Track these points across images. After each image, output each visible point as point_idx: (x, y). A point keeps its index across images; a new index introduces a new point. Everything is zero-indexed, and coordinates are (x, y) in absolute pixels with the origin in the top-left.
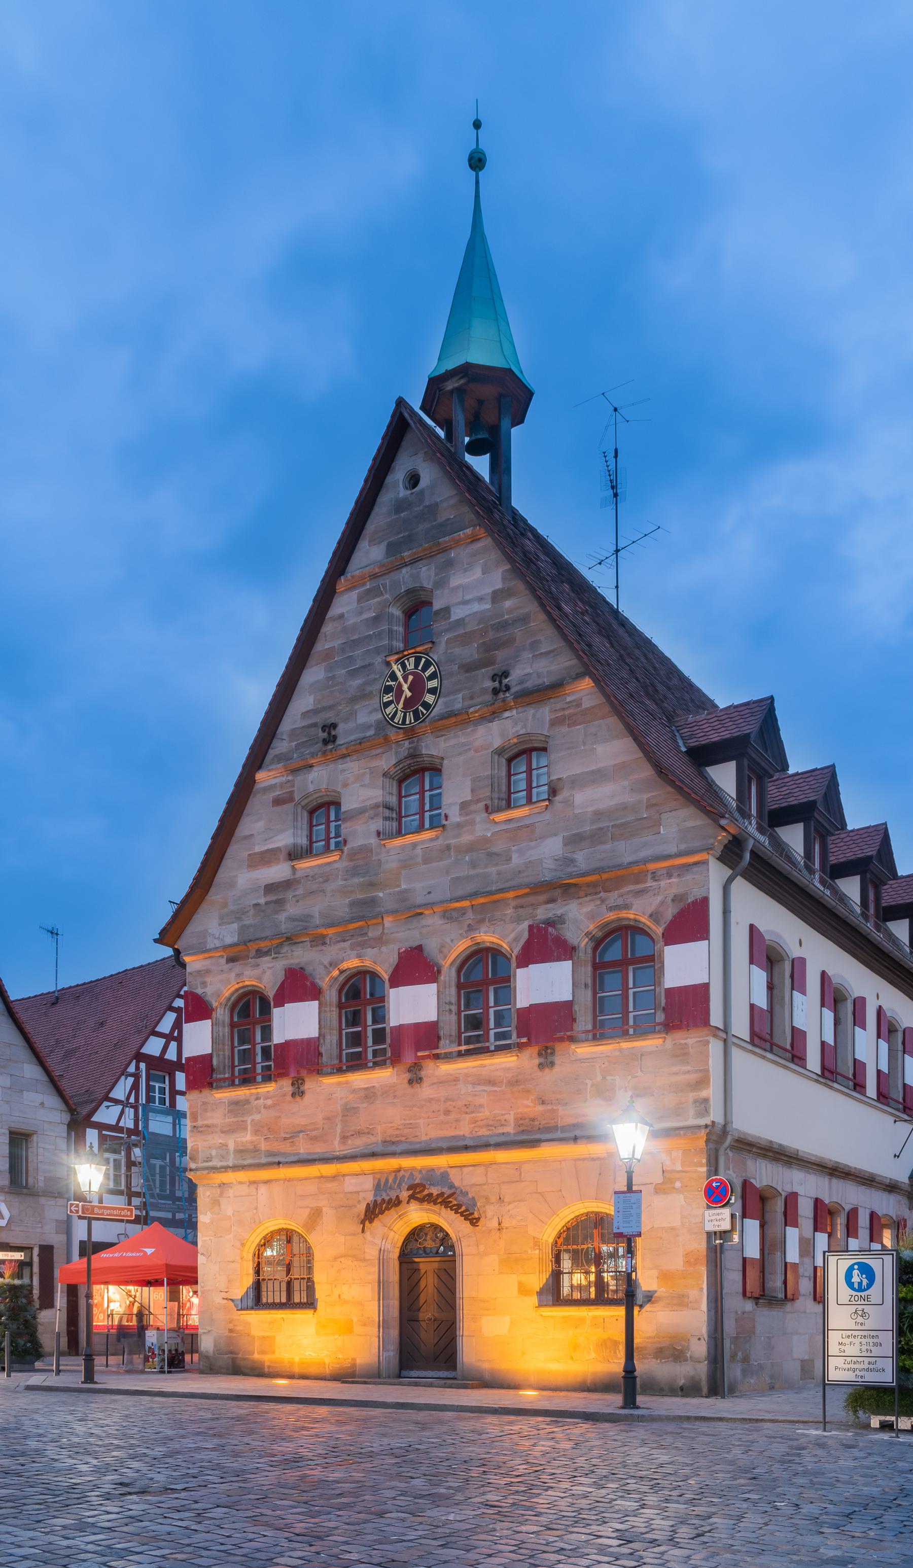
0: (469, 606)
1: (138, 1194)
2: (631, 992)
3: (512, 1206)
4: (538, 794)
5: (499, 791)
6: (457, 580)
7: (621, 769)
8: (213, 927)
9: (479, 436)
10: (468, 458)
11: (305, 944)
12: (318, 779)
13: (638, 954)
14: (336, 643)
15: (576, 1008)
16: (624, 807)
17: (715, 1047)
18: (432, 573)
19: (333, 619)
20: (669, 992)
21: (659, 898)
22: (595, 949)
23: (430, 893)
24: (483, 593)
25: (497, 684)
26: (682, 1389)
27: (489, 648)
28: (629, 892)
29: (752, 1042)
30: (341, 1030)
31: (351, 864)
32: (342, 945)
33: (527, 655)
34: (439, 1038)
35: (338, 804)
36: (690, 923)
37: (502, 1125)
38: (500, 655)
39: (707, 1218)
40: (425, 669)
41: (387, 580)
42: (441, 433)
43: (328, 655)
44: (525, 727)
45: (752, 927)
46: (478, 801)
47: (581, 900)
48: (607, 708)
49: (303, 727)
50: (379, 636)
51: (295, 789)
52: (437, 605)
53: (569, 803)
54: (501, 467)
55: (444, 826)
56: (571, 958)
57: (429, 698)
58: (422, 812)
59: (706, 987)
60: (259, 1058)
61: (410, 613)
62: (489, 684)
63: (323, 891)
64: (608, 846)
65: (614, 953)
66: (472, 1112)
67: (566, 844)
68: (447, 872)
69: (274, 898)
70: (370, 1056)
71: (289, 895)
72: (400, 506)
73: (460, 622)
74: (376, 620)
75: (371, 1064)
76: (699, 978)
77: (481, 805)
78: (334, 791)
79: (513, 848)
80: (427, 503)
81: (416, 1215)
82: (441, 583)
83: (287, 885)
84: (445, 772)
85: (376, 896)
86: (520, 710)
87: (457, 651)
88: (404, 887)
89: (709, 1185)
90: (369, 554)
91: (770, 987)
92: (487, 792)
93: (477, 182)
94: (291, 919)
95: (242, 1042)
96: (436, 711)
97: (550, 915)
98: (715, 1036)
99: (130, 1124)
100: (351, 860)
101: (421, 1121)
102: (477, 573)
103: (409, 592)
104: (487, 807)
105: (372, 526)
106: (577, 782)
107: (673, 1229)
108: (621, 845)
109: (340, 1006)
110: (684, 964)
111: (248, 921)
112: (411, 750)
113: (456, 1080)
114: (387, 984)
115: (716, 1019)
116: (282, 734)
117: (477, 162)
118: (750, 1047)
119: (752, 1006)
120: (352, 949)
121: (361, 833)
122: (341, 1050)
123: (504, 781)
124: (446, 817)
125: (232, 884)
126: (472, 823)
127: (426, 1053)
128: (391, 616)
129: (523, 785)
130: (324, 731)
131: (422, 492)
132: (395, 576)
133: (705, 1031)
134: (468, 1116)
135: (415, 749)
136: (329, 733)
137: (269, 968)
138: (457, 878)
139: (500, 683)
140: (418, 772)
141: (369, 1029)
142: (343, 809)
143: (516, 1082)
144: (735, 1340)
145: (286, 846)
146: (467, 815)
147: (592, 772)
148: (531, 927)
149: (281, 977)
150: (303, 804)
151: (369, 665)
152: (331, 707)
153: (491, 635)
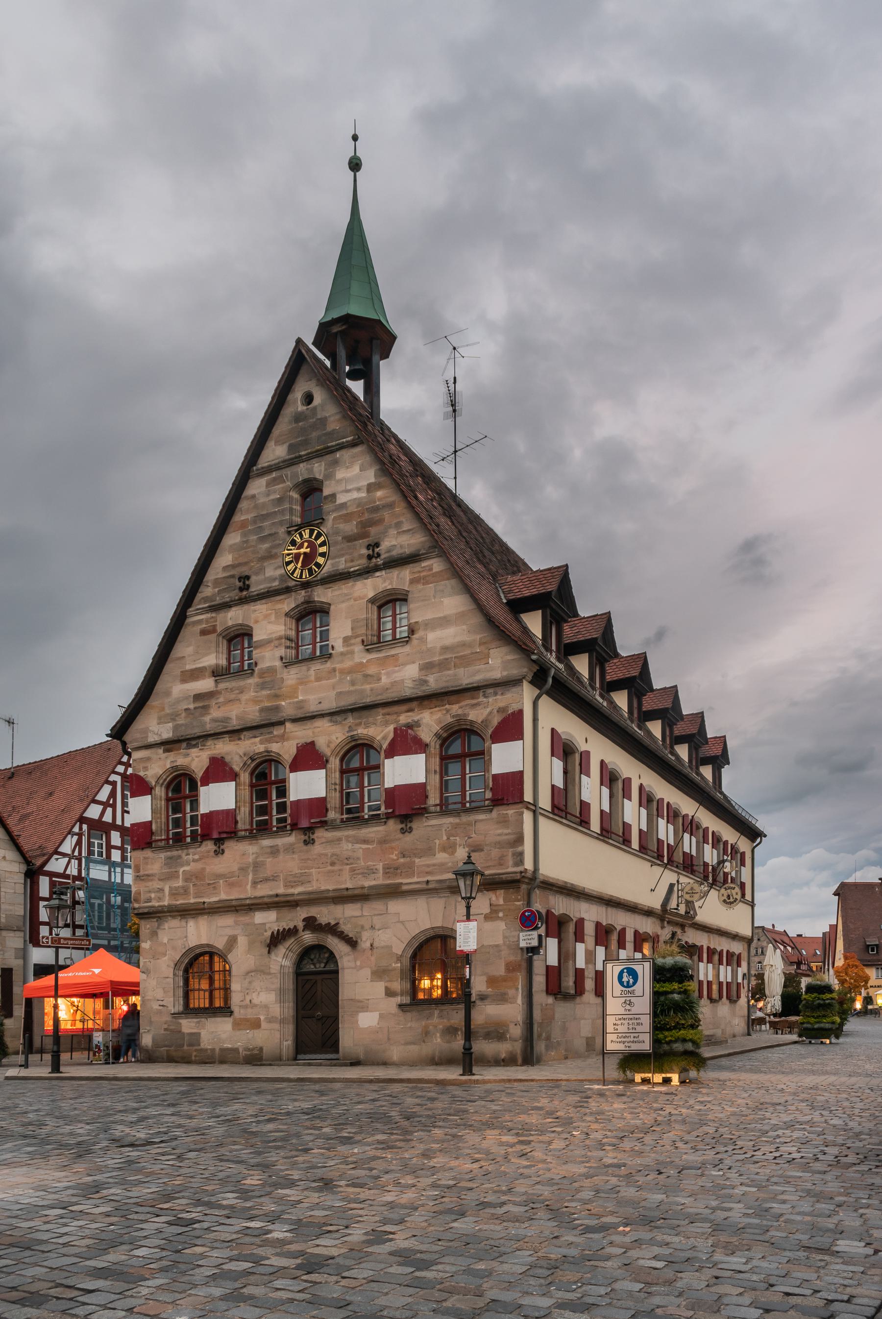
0: (350, 494)
1: (81, 927)
2: (468, 776)
4: (400, 632)
5: (372, 629)
6: (340, 474)
7: (460, 617)
8: (153, 726)
9: (357, 367)
10: (349, 383)
12: (234, 617)
13: (473, 749)
14: (249, 516)
15: (428, 788)
16: (463, 645)
17: (528, 817)
18: (323, 468)
19: (247, 498)
20: (495, 777)
21: (488, 710)
22: (441, 746)
24: (360, 484)
25: (370, 552)
26: (503, 1060)
27: (365, 525)
28: (466, 705)
29: (553, 812)
30: (252, 803)
31: (261, 680)
33: (393, 532)
34: (327, 810)
35: (250, 635)
36: (510, 728)
38: (373, 530)
39: (521, 938)
40: (317, 538)
41: (288, 472)
42: (328, 363)
43: (244, 524)
44: (391, 583)
45: (553, 730)
50: (282, 512)
52: (326, 492)
53: (423, 640)
54: (372, 390)
55: (331, 654)
56: (425, 752)
57: (320, 560)
58: (314, 644)
59: (521, 774)
60: (188, 825)
61: (305, 496)
62: (364, 551)
63: (239, 700)
65: (456, 748)
66: (352, 864)
67: (421, 670)
68: (334, 688)
69: (201, 704)
70: (275, 823)
71: (213, 702)
72: (298, 418)
73: (343, 505)
74: (280, 501)
75: (275, 829)
76: (518, 767)
77: (359, 640)
78: (248, 626)
80: (319, 417)
81: (308, 938)
82: (329, 476)
83: (210, 695)
84: (331, 613)
86: (388, 571)
87: (341, 526)
88: (300, 698)
89: (523, 914)
90: (275, 452)
91: (565, 772)
92: (363, 631)
94: (214, 720)
95: (174, 812)
96: (326, 569)
97: (410, 721)
98: (528, 808)
99: (75, 872)
100: (260, 677)
101: (313, 870)
102: (356, 469)
103: (306, 481)
104: (363, 641)
105: (277, 431)
106: (431, 625)
107: (497, 946)
108: (461, 671)
109: (252, 786)
110: (505, 758)
111: (181, 721)
113: (339, 839)
114: (288, 769)
115: (528, 797)
116: (208, 582)
118: (551, 816)
119: (553, 786)
120: (261, 743)
121: (269, 658)
122: (252, 818)
123: (376, 622)
124: (333, 647)
125: (168, 694)
126: (352, 653)
127: (318, 820)
128: (291, 498)
129: (389, 626)
130: (240, 581)
131: (315, 408)
132: (294, 469)
133: (520, 805)
135: (309, 596)
136: (244, 583)
138: (341, 693)
139: (373, 551)
140: (311, 613)
141: (274, 803)
142: (255, 639)
143: (383, 841)
144: (540, 1025)
145: (210, 666)
146: (348, 646)
147: (440, 618)
148: (395, 729)
149: (206, 763)
152: (246, 563)
153: (367, 516)
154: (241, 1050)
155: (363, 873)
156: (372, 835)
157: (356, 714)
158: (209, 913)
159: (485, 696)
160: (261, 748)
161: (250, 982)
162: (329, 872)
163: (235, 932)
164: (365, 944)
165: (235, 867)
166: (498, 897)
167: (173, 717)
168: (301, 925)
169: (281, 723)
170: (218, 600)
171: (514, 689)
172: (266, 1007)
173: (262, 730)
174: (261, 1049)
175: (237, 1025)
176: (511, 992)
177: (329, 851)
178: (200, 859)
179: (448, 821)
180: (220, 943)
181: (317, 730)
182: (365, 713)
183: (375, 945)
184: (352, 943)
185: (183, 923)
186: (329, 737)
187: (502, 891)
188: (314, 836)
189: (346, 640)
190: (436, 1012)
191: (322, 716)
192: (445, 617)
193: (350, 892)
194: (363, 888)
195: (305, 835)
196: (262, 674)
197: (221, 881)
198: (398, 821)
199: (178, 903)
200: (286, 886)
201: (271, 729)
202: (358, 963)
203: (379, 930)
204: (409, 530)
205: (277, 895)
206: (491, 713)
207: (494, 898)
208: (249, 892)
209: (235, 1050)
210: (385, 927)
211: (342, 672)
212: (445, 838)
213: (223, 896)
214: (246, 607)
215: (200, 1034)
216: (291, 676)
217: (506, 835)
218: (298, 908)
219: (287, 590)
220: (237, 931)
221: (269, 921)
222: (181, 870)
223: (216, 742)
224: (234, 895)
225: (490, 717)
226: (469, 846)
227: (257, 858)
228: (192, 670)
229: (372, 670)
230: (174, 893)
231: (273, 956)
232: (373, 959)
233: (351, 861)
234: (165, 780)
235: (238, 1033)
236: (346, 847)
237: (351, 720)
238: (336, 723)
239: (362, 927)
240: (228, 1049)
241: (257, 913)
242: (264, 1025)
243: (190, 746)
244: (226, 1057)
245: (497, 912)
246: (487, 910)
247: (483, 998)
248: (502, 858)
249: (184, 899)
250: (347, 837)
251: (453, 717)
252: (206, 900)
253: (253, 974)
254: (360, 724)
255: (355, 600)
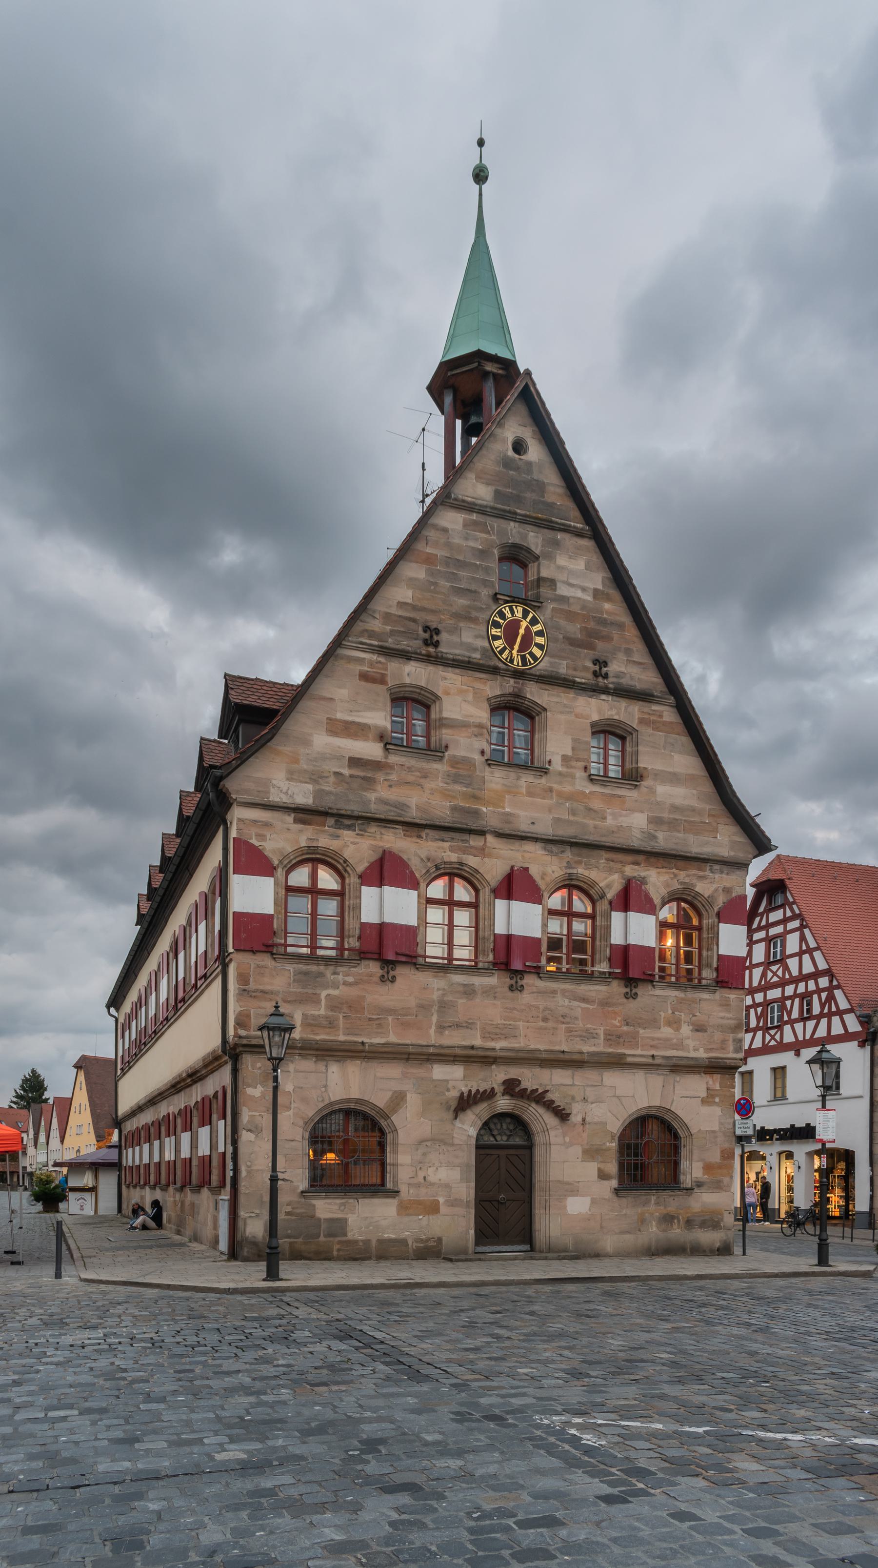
0: (573, 590)
3: (594, 1105)
11: (398, 831)
12: (414, 674)
16: (693, 810)
21: (714, 886)
23: (533, 823)
32: (441, 844)
37: (594, 1038)
41: (496, 523)
43: (429, 560)
46: (578, 760)
47: (659, 870)
48: (681, 728)
49: (400, 616)
51: (388, 673)
64: (680, 835)
66: (568, 1023)
69: (362, 774)
71: (380, 776)
73: (564, 599)
79: (608, 811)
81: (503, 1104)
83: (377, 766)
85: (480, 809)
86: (615, 698)
88: (507, 810)
93: (481, 195)
97: (635, 874)
101: (521, 1023)
103: (515, 546)
107: (713, 1132)
108: (691, 838)
111: (329, 786)
112: (516, 690)
113: (554, 992)
117: (480, 176)
120: (452, 849)
125: (306, 742)
129: (611, 760)
134: (564, 1026)
137: (352, 843)
138: (558, 819)
147: (670, 773)
150: (393, 691)
151: (475, 592)
152: (433, 612)
154: (410, 1242)
155: (581, 1036)
156: (593, 994)
157: (575, 850)
158: (365, 1057)
159: (712, 871)
160: (453, 857)
161: (424, 1154)
162: (541, 1028)
163: (404, 1088)
164: (576, 1118)
165: (412, 1003)
166: (715, 1082)
167: (315, 777)
168: (499, 1089)
169: (481, 833)
170: (390, 642)
171: (738, 872)
172: (447, 1186)
173: (452, 834)
174: (440, 1240)
175: (405, 1209)
176: (726, 1180)
177: (542, 1003)
178: (356, 983)
179: (674, 993)
180: (380, 1100)
181: (527, 855)
182: (585, 851)
183: (587, 1119)
184: (562, 1115)
185: (321, 1066)
186: (545, 866)
187: (719, 1076)
188: (524, 982)
189: (565, 759)
190: (653, 1198)
191: (536, 840)
192: (674, 774)
193: (567, 1057)
194: (581, 1053)
195: (511, 978)
196: (455, 762)
197: (390, 1018)
198: (622, 983)
199: (318, 1038)
200: (483, 1038)
201: (466, 837)
202: (567, 1139)
203: (592, 1103)
204: (640, 663)
205: (473, 1048)
206: (716, 890)
207: (711, 1083)
208: (431, 1037)
209: (403, 1242)
210: (599, 1101)
211: (560, 794)
212: (670, 1012)
213: (393, 1038)
214: (431, 668)
215: (346, 1220)
216: (496, 779)
217: (728, 1019)
218: (494, 1067)
219: (494, 671)
220: (407, 1086)
221: (454, 1078)
222: (324, 994)
223: (383, 831)
224: (410, 1038)
225: (715, 894)
226: (693, 1024)
227: (444, 995)
228: (346, 723)
229: (596, 804)
230: (310, 1023)
231: (458, 1123)
232: (585, 1135)
233: (567, 1020)
234: (291, 861)
235: (406, 1219)
236: (562, 1003)
237: (568, 854)
238: (551, 852)
239: (573, 1098)
240: (390, 1241)
241: (435, 1066)
242: (443, 1209)
243: (339, 825)
244: (387, 1251)
245: (713, 1096)
246: (704, 1094)
247: (700, 1184)
248: (724, 1041)
249: (328, 1034)
250: (564, 991)
251: (681, 883)
252: (366, 1040)
253: (429, 1144)
254: (580, 862)
255: (577, 716)
